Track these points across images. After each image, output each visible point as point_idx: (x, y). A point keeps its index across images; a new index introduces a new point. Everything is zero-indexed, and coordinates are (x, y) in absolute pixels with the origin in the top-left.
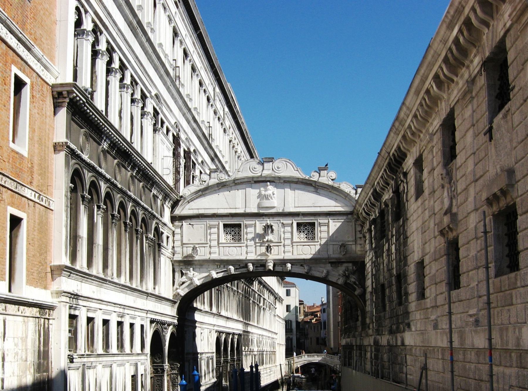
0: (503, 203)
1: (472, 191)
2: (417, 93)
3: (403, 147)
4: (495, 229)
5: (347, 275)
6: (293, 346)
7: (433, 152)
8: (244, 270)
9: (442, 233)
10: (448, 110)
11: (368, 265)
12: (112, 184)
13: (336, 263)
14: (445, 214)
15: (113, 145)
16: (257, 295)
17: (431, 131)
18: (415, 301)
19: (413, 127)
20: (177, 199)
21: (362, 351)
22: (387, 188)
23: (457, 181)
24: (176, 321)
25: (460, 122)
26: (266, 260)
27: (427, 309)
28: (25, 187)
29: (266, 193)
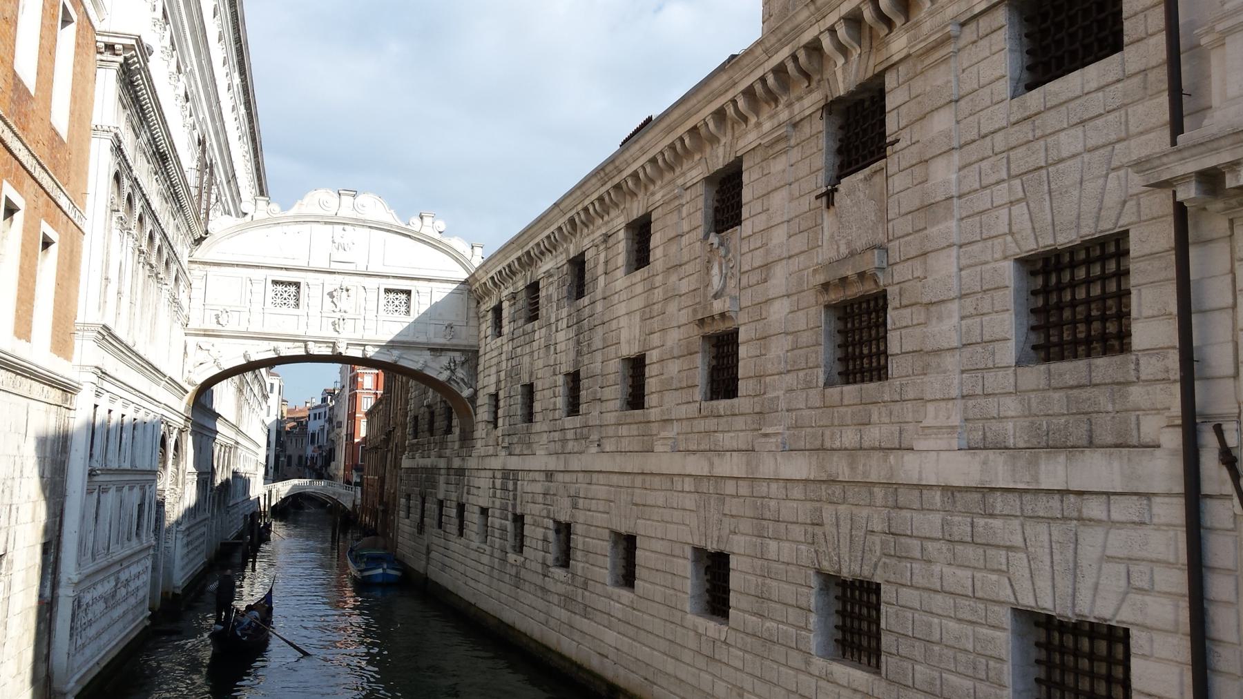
0: (855, 291)
1: (780, 272)
2: (671, 129)
3: (611, 199)
4: (826, 323)
5: (453, 368)
6: (269, 468)
7: (680, 212)
8: (301, 352)
9: (702, 322)
10: (732, 159)
11: (488, 356)
12: (147, 201)
13: (437, 350)
14: (716, 296)
15: (153, 140)
16: (249, 388)
17: (680, 182)
18: (616, 411)
19: (641, 175)
20: (201, 237)
21: (464, 476)
22: (551, 252)
23: (742, 255)
24: (182, 422)
25: (755, 176)
26: (336, 339)
27: (649, 422)
28: (62, 190)
29: (342, 241)
